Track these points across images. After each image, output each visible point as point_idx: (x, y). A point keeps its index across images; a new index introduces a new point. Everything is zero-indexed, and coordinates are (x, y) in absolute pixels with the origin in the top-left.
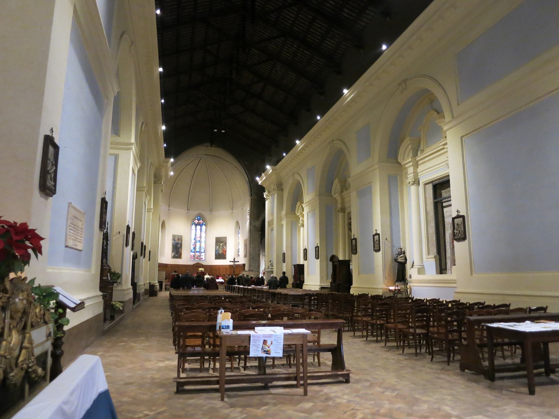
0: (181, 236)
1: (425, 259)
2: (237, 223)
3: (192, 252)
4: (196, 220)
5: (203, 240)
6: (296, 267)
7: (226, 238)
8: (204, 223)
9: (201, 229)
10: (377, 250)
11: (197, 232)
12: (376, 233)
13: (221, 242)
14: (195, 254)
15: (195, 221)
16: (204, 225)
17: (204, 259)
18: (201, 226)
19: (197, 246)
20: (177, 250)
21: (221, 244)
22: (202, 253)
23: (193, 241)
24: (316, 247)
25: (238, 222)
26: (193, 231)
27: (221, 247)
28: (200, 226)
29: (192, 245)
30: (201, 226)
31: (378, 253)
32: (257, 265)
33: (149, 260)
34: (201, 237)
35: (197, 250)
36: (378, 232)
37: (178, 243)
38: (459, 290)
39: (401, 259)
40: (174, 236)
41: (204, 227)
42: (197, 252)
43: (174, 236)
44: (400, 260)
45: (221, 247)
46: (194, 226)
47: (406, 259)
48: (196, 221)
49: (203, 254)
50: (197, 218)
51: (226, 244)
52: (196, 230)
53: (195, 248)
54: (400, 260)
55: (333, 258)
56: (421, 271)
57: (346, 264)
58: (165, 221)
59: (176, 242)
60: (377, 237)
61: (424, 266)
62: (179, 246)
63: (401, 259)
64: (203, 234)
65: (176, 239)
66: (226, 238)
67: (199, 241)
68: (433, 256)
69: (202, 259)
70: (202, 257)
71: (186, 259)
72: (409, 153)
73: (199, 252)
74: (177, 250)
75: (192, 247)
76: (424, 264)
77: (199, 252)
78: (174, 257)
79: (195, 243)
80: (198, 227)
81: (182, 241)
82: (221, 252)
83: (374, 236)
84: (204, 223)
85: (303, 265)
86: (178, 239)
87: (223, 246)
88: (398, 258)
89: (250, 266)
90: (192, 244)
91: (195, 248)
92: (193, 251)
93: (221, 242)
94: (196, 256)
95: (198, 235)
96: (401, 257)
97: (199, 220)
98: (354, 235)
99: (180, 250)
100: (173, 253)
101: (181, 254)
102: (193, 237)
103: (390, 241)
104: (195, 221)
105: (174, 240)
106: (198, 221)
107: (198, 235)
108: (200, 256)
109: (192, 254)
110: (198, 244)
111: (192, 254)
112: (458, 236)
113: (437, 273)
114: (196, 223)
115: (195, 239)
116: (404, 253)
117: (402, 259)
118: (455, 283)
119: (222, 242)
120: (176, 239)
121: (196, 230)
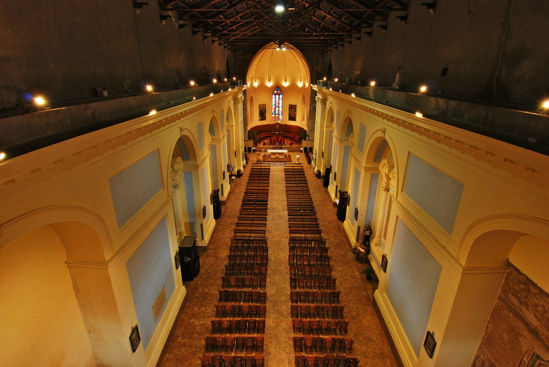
0: (265, 105)
2: (304, 97)
3: (273, 114)
4: (276, 91)
5: (280, 105)
7: (296, 105)
8: (281, 93)
9: (279, 98)
11: (276, 100)
13: (292, 109)
14: (275, 116)
15: (275, 92)
17: (281, 119)
19: (277, 110)
20: (263, 115)
21: (293, 110)
22: (280, 115)
23: (274, 106)
25: (304, 97)
26: (274, 99)
27: (293, 112)
29: (273, 110)
34: (279, 104)
35: (277, 113)
37: (263, 110)
40: (260, 106)
41: (281, 96)
42: (276, 114)
43: (260, 106)
45: (293, 112)
46: (274, 95)
48: (275, 92)
49: (281, 116)
50: (276, 89)
51: (296, 110)
52: (275, 98)
53: (275, 112)
54: (367, 233)
58: (253, 97)
59: (261, 109)
62: (264, 112)
64: (281, 102)
65: (262, 107)
66: (296, 105)
67: (278, 106)
69: (280, 119)
70: (280, 118)
71: (269, 121)
72: (386, 168)
73: (278, 114)
74: (263, 115)
75: (273, 111)
77: (278, 114)
78: (261, 120)
79: (275, 107)
80: (277, 96)
81: (266, 108)
82: (292, 116)
84: (281, 93)
86: (263, 107)
87: (294, 112)
90: (273, 108)
91: (275, 112)
92: (274, 113)
93: (292, 109)
94: (276, 117)
95: (277, 102)
97: (277, 91)
99: (265, 114)
100: (260, 118)
101: (265, 117)
102: (274, 103)
104: (275, 92)
105: (260, 108)
106: (277, 92)
107: (277, 102)
108: (279, 117)
109: (273, 116)
110: (277, 109)
111: (273, 116)
114: (276, 93)
115: (275, 105)
117: (368, 234)
119: (294, 109)
120: (262, 107)
121: (275, 98)
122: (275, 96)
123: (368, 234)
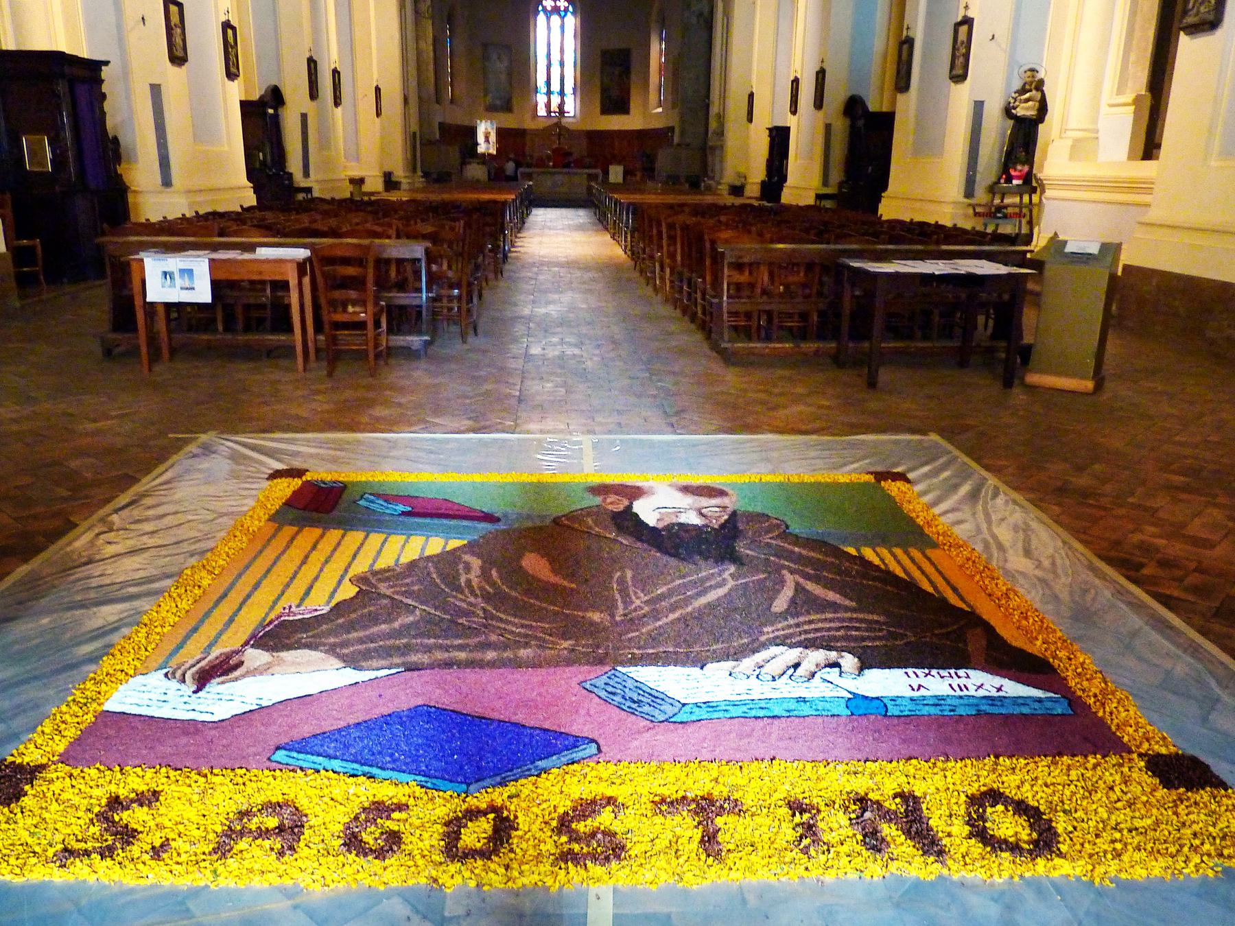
1: (1104, 109)
6: (774, 133)
10: (958, 76)
12: (965, 17)
16: (569, 14)
18: (563, 18)
24: (818, 73)
28: (560, 15)
30: (563, 18)
31: (960, 87)
32: (702, 130)
33: (378, 114)
36: (970, 14)
38: (1153, 215)
39: (1023, 108)
44: (1020, 112)
47: (1043, 108)
54: (1026, 110)
55: (854, 106)
56: (1080, 149)
57: (886, 122)
60: (964, 29)
61: (1097, 131)
63: (1023, 108)
68: (1129, 97)
76: (1100, 125)
80: (555, 19)
83: (958, 25)
85: (788, 129)
88: (1017, 103)
89: (683, 133)
96: (1027, 100)
98: (908, 28)
103: (1004, 46)
112: (1197, 13)
113: (1131, 157)
116: (1039, 85)
117: (1027, 109)
118: (1149, 191)
122: (548, 19)
123: (1027, 109)
